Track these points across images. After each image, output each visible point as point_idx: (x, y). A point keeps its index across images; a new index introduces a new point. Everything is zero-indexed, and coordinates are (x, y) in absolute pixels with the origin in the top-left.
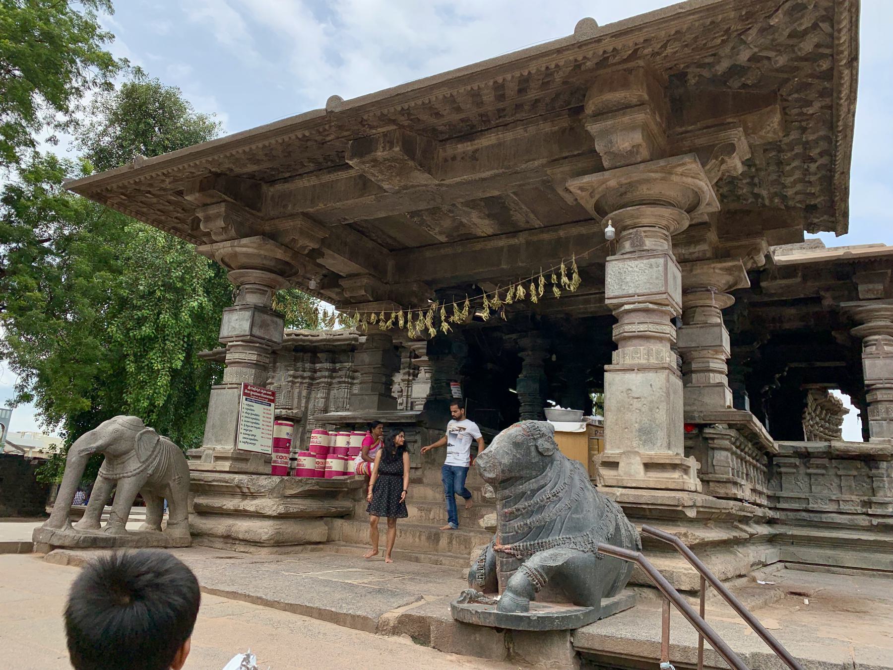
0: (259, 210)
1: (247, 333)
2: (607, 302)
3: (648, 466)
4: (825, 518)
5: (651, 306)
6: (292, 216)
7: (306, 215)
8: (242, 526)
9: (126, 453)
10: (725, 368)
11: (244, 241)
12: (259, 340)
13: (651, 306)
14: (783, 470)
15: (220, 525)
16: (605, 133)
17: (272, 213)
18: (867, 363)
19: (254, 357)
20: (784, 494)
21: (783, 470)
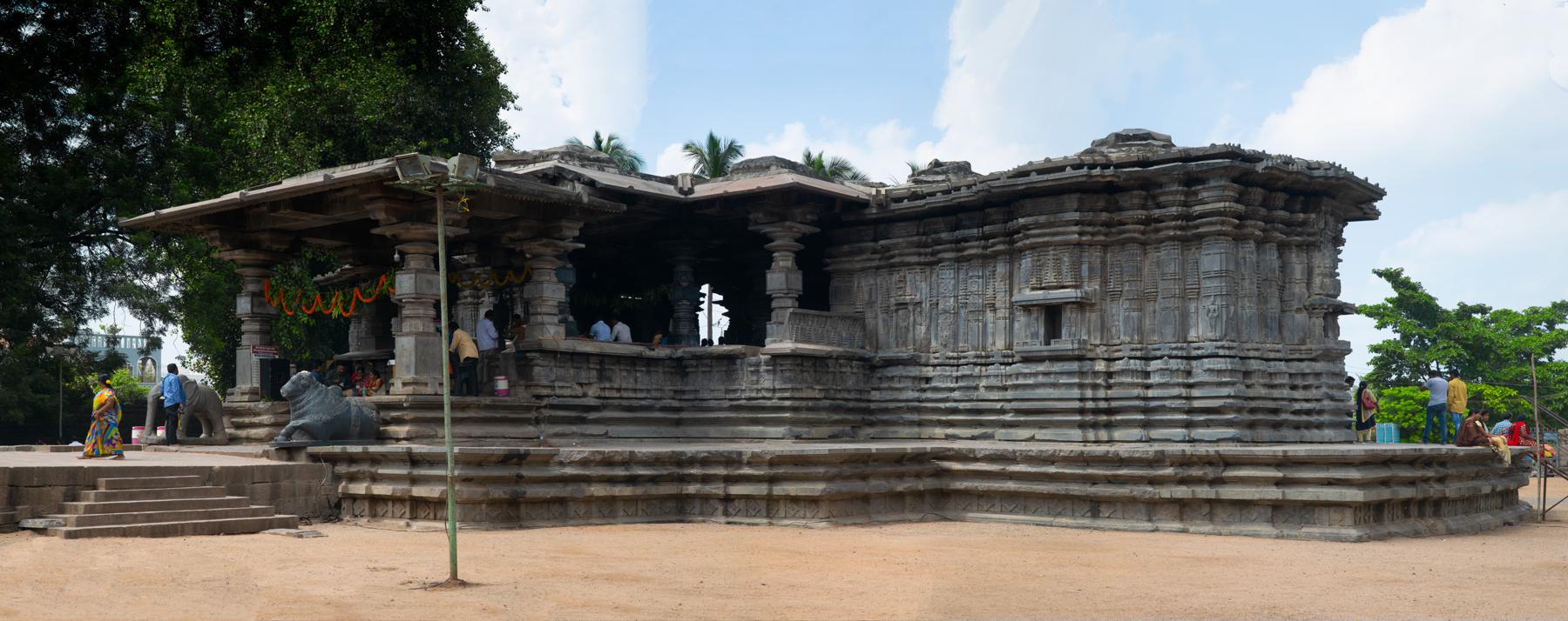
3: (404, 384)
4: (705, 404)
7: (272, 230)
8: (253, 432)
10: (556, 311)
15: (242, 433)
18: (769, 276)
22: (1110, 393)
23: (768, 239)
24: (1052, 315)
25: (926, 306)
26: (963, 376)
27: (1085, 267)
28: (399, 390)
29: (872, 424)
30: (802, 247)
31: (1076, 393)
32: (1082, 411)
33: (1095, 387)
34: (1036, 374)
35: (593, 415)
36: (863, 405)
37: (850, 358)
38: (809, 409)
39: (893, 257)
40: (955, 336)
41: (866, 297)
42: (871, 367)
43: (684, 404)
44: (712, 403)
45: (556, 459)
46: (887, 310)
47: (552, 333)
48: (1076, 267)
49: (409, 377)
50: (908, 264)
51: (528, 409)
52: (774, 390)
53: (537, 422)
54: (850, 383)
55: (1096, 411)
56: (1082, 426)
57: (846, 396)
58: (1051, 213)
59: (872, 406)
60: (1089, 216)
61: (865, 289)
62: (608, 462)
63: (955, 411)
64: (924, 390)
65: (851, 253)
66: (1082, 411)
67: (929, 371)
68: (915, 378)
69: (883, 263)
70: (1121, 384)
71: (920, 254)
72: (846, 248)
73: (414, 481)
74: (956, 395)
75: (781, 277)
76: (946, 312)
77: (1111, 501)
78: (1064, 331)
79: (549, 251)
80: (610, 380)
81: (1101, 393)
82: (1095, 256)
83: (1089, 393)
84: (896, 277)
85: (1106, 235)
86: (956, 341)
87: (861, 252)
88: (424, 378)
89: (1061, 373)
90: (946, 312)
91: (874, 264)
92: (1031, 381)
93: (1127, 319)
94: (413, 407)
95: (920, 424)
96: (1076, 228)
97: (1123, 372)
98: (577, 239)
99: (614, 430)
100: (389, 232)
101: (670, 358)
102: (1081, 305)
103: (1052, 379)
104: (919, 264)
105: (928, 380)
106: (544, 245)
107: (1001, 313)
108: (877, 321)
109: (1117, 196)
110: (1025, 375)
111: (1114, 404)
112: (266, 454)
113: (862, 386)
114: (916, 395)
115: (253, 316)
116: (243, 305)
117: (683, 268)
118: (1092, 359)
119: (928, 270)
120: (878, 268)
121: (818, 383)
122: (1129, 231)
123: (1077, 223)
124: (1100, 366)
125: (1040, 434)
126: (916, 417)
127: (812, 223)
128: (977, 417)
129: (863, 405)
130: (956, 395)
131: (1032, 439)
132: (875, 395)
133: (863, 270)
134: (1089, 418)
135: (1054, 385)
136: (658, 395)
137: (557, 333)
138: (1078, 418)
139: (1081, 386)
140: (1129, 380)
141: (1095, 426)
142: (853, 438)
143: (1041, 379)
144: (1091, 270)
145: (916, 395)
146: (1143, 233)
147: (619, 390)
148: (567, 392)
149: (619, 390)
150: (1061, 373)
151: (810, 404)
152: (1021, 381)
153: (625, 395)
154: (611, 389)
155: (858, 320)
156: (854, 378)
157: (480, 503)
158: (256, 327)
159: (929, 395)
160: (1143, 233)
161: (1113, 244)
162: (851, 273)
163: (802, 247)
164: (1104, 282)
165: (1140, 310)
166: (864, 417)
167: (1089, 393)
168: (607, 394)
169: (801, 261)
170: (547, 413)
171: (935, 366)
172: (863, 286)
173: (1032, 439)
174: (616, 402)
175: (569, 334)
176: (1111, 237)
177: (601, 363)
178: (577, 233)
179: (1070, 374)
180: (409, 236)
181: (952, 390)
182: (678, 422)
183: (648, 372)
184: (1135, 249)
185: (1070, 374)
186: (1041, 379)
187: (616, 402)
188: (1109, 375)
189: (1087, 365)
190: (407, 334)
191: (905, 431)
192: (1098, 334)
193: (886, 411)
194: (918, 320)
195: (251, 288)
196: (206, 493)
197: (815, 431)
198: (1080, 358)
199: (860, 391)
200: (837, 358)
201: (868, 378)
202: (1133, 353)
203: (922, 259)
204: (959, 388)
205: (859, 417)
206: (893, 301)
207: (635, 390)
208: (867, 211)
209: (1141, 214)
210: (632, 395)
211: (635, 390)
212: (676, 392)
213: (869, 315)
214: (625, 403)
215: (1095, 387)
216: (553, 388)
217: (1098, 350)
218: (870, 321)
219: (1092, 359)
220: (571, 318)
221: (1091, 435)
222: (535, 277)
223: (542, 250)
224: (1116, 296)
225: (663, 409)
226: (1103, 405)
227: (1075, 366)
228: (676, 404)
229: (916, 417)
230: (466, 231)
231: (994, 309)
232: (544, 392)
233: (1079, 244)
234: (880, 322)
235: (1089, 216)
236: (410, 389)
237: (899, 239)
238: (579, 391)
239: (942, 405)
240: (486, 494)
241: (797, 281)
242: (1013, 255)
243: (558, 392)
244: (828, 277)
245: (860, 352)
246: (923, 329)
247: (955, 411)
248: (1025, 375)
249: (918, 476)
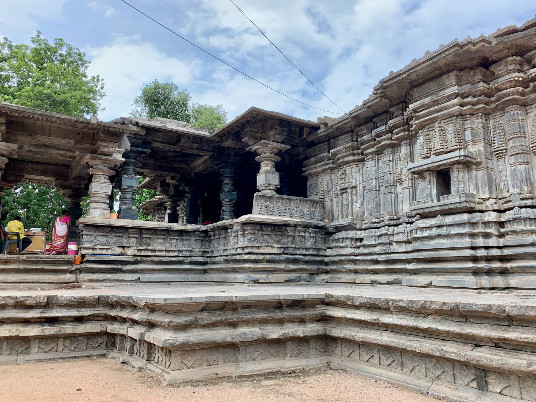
18: (258, 177)
22: (502, 242)
23: (256, 154)
24: (443, 177)
25: (360, 189)
26: (381, 235)
27: (468, 133)
29: (327, 272)
30: (279, 158)
31: (467, 241)
32: (475, 259)
33: (487, 236)
34: (430, 228)
36: (318, 259)
37: (307, 226)
38: (269, 261)
39: (339, 159)
40: (378, 207)
41: (325, 189)
42: (327, 233)
43: (208, 260)
44: (218, 259)
46: (337, 196)
48: (460, 134)
50: (348, 163)
52: (243, 248)
54: (309, 244)
55: (489, 259)
56: (476, 272)
57: (304, 252)
58: (433, 94)
59: (326, 259)
60: (467, 88)
61: (325, 183)
62: (20, 305)
63: (377, 262)
64: (358, 247)
65: (317, 162)
66: (475, 259)
67: (360, 234)
68: (352, 239)
69: (335, 166)
70: (513, 232)
71: (354, 155)
72: (313, 159)
74: (377, 249)
75: (267, 177)
76: (370, 190)
77: (502, 373)
78: (453, 189)
81: (493, 242)
82: (477, 123)
83: (480, 242)
84: (341, 172)
85: (487, 104)
86: (378, 210)
87: (322, 160)
89: (453, 225)
90: (370, 190)
91: (328, 166)
92: (426, 234)
93: (514, 174)
95: (356, 272)
96: (457, 100)
97: (514, 220)
99: (142, 277)
102: (467, 164)
103: (444, 230)
104: (354, 161)
105: (361, 240)
107: (405, 184)
108: (333, 204)
109: (492, 68)
110: (422, 229)
111: (506, 252)
113: (319, 245)
114: (353, 250)
118: (482, 212)
119: (361, 165)
120: (332, 169)
121: (278, 242)
122: (508, 95)
123: (457, 95)
124: (492, 217)
125: (436, 280)
126: (352, 267)
127: (282, 142)
128: (390, 267)
129: (318, 259)
130: (377, 249)
131: (430, 285)
132: (329, 252)
133: (324, 171)
134: (482, 265)
135: (446, 236)
136: (188, 254)
138: (470, 265)
139: (472, 235)
140: (522, 227)
141: (489, 272)
142: (309, 282)
143: (435, 231)
144: (474, 135)
145: (353, 250)
146: (523, 94)
150: (453, 225)
151: (268, 257)
152: (419, 234)
153: (158, 254)
155: (321, 203)
156: (312, 240)
159: (362, 250)
160: (523, 94)
161: (494, 110)
162: (317, 174)
163: (279, 158)
164: (488, 143)
165: (528, 163)
166: (319, 266)
167: (480, 242)
168: (143, 253)
169: (278, 167)
171: (365, 230)
172: (324, 180)
173: (430, 285)
174: (149, 259)
176: (493, 105)
179: (460, 224)
181: (375, 246)
182: (205, 272)
184: (515, 112)
185: (460, 224)
186: (435, 231)
187: (149, 259)
188: (502, 224)
189: (476, 217)
191: (346, 277)
192: (487, 189)
193: (334, 262)
194: (355, 198)
197: (272, 277)
198: (470, 211)
199: (318, 249)
200: (295, 226)
201: (325, 241)
202: (524, 203)
203: (356, 158)
204: (379, 244)
205: (315, 267)
206: (339, 188)
208: (319, 131)
209: (517, 76)
212: (204, 252)
213: (327, 199)
214: (155, 259)
215: (487, 236)
217: (488, 203)
218: (328, 204)
219: (482, 212)
221: (485, 281)
224: (500, 154)
225: (191, 263)
226: (495, 252)
227: (465, 217)
229: (352, 267)
231: (401, 182)
233: (461, 115)
234: (335, 204)
235: (467, 88)
237: (342, 147)
238: (120, 250)
239: (368, 258)
241: (275, 179)
242: (411, 139)
244: (305, 180)
245: (322, 224)
246: (358, 204)
247: (377, 262)
248: (422, 229)
249: (302, 321)
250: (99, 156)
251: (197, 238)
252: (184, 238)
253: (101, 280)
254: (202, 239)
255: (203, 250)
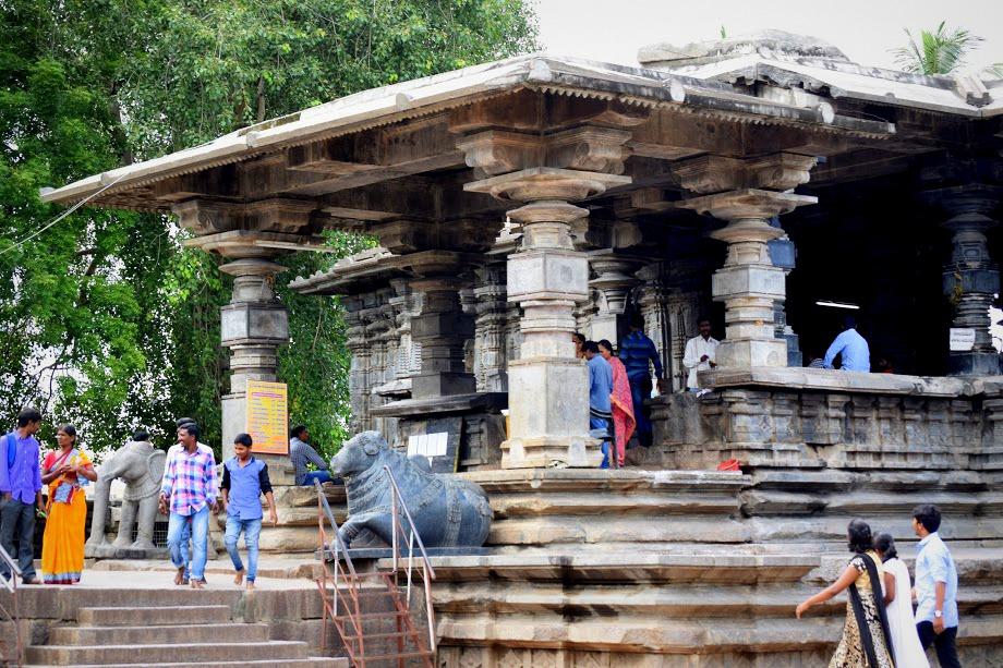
0: (237, 193)
1: (245, 335)
2: (509, 300)
3: (528, 449)
5: (538, 303)
6: (270, 198)
7: (283, 196)
9: (140, 477)
10: (770, 316)
11: (225, 235)
12: (261, 341)
13: (538, 303)
14: (994, 417)
16: (470, 150)
17: (251, 194)
19: (258, 361)
20: (990, 450)
21: (994, 417)
28: (516, 461)
35: (835, 501)
43: (988, 479)
45: (813, 575)
47: (765, 354)
49: (537, 437)
51: (732, 490)
53: (745, 514)
73: (572, 613)
79: (757, 210)
80: (862, 437)
88: (559, 438)
94: (550, 488)
98: (801, 189)
100: (494, 186)
101: (962, 397)
106: (752, 201)
112: (306, 572)
115: (251, 344)
116: (234, 325)
117: (970, 235)
137: (773, 355)
147: (878, 455)
148: (793, 460)
149: (878, 455)
153: (889, 463)
154: (867, 453)
157: (694, 651)
158: (255, 360)
168: (860, 462)
170: (759, 497)
174: (875, 477)
175: (791, 359)
177: (848, 407)
178: (805, 177)
180: (533, 193)
183: (926, 422)
187: (875, 477)
190: (531, 363)
195: (246, 294)
196: (239, 633)
207: (905, 455)
210: (872, 463)
211: (905, 455)
212: (972, 456)
214: (890, 478)
216: (770, 451)
220: (788, 330)
222: (734, 257)
223: (744, 209)
225: (954, 488)
228: (975, 479)
230: (628, 180)
232: (755, 460)
236: (538, 458)
240: (700, 637)
243: (778, 460)
250: (770, 194)
251: (955, 417)
252: (931, 417)
253: (796, 536)
254: (967, 418)
255: (970, 451)
